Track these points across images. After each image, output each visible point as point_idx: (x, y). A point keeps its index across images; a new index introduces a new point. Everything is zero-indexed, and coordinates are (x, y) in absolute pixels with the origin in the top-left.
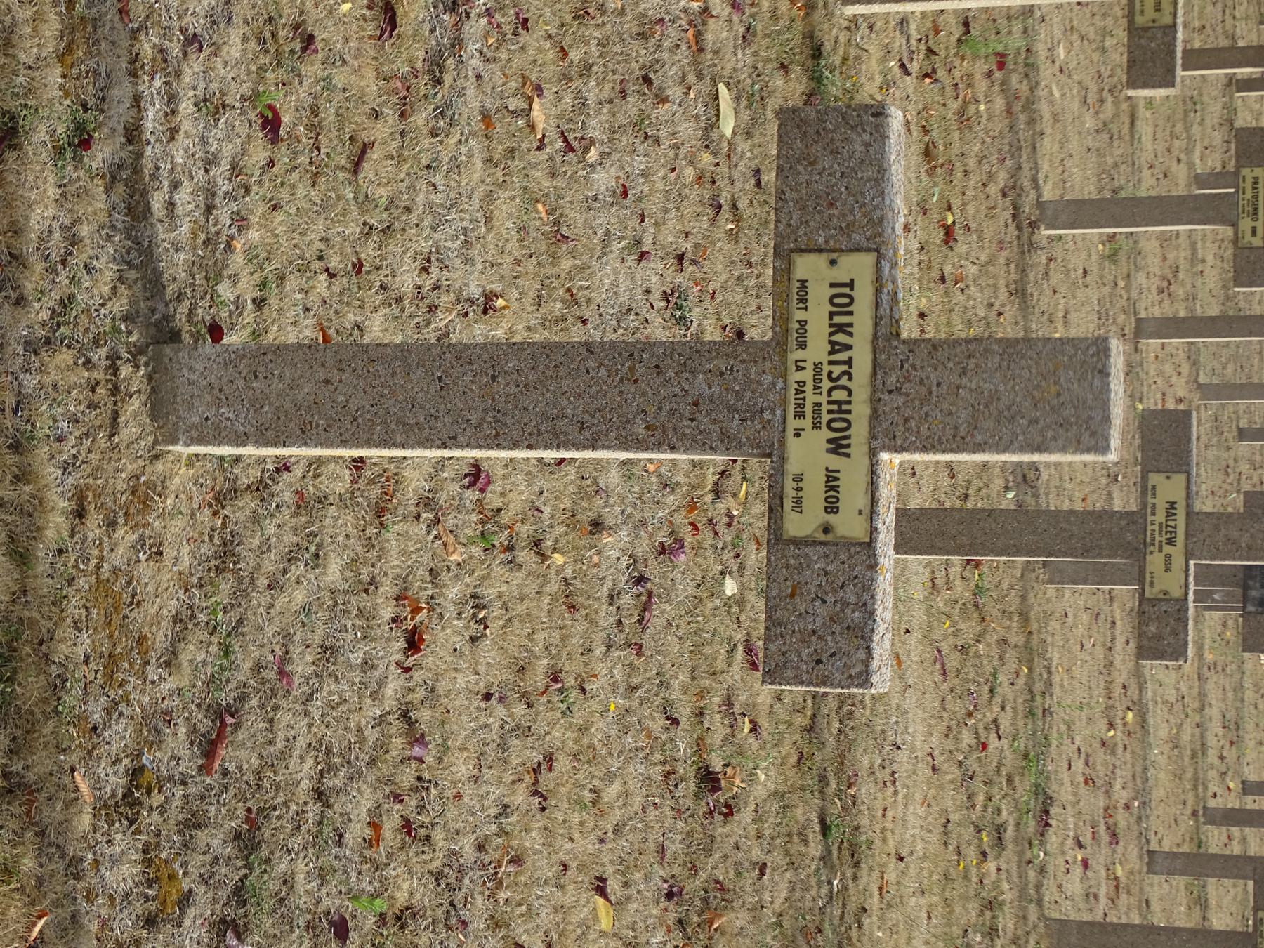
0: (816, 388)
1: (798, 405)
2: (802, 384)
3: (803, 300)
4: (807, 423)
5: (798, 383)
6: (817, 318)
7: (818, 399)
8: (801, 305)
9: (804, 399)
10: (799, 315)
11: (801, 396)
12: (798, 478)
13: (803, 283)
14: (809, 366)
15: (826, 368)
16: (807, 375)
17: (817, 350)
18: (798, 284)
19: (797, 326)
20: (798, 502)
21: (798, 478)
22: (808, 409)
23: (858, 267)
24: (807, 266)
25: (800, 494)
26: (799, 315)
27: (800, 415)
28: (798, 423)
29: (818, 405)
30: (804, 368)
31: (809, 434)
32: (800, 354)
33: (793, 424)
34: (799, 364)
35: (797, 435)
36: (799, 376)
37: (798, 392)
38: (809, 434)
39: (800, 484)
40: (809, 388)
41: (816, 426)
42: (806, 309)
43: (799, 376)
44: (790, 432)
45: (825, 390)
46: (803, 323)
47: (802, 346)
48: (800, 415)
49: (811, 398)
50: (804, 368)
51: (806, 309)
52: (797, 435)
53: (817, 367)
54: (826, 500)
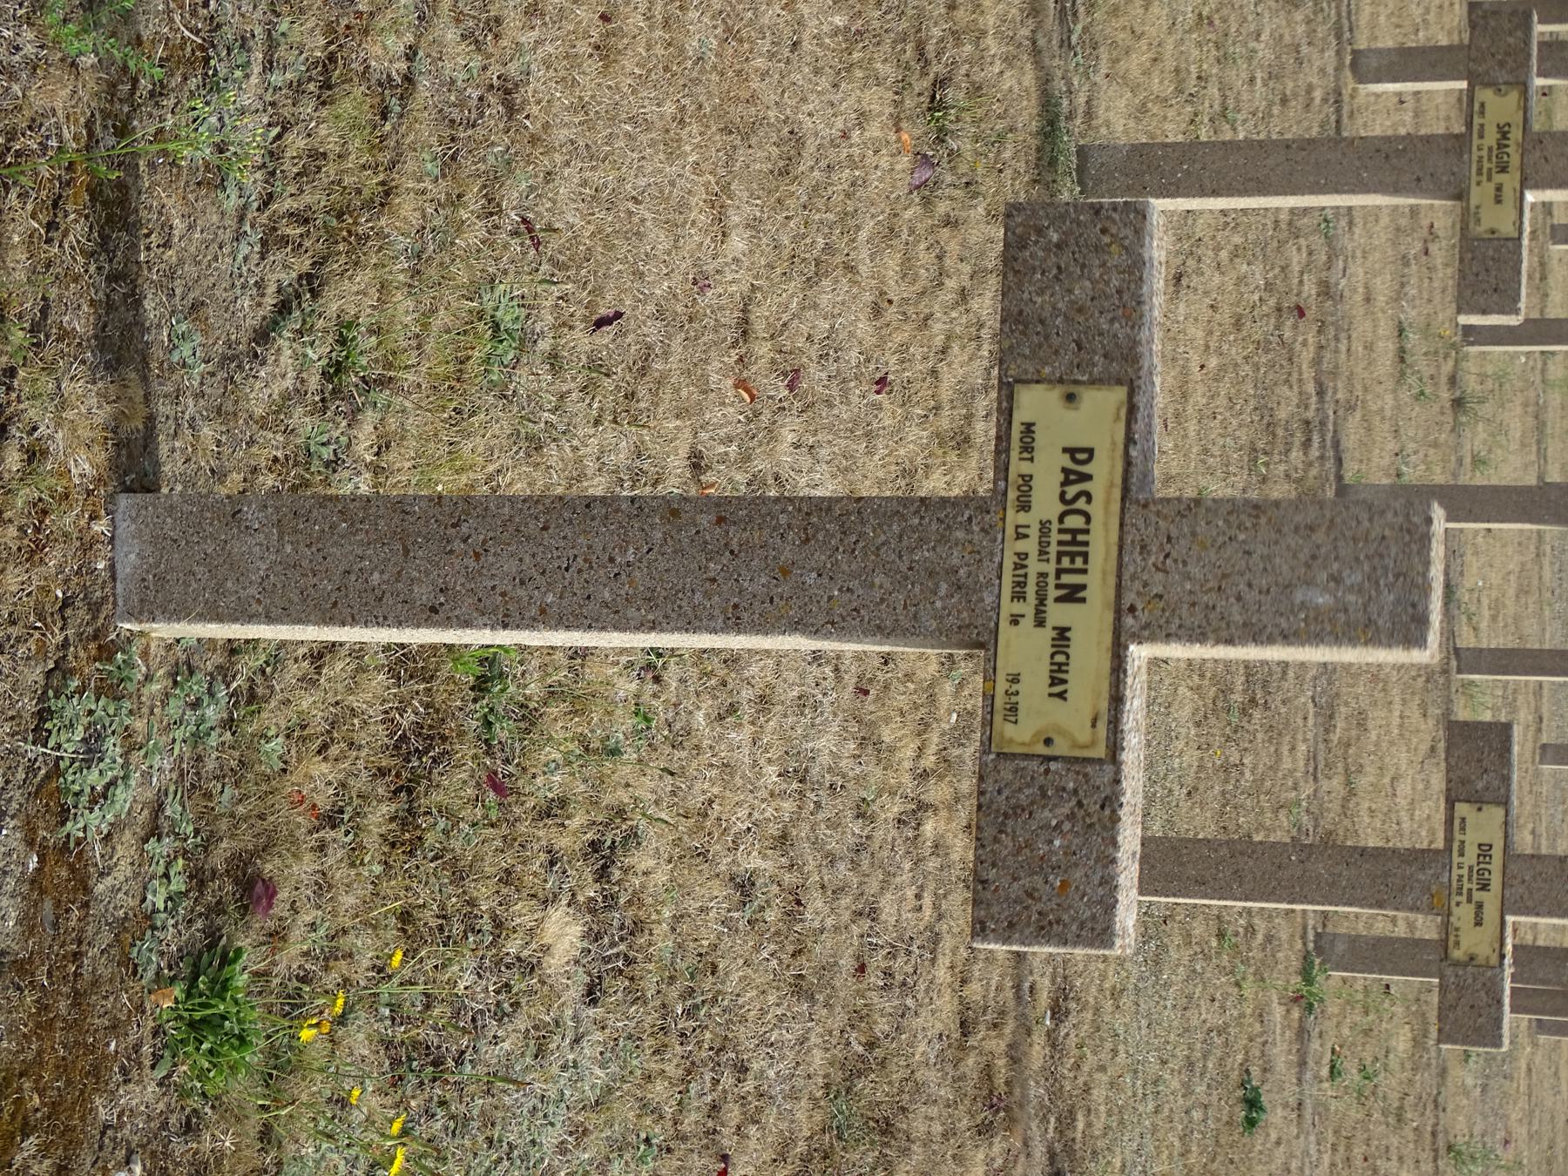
1: (1018, 584)
2: (1023, 556)
3: (1028, 448)
5: (1018, 554)
6: (1046, 471)
8: (1026, 455)
9: (1025, 576)
12: (1015, 679)
13: (1029, 428)
18: (1023, 428)
19: (1020, 481)
20: (1013, 709)
21: (1015, 679)
24: (1034, 403)
25: (1014, 699)
26: (1025, 468)
30: (1026, 536)
32: (1022, 518)
33: (1008, 607)
34: (1020, 530)
37: (1017, 566)
39: (1015, 687)
42: (1032, 459)
43: (1021, 546)
44: (1004, 624)
46: (1027, 479)
50: (1026, 536)
51: (1032, 459)
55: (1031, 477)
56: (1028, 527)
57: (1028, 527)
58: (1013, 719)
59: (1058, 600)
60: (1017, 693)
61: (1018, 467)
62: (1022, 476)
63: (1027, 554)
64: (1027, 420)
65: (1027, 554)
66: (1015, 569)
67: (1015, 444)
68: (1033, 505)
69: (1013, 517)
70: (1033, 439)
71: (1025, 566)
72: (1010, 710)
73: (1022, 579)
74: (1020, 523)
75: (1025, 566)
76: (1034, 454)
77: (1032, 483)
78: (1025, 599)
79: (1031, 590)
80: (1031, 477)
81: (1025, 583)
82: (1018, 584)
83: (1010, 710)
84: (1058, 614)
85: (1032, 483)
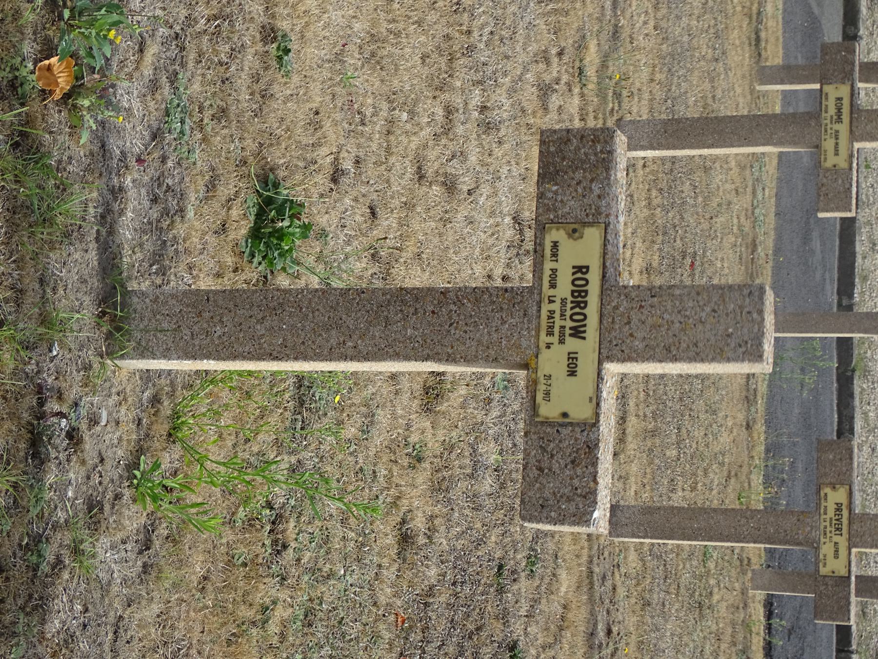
0: (562, 315)
2: (552, 312)
3: (555, 255)
4: (555, 339)
5: (550, 311)
7: (563, 323)
8: (554, 258)
9: (554, 323)
10: (553, 265)
11: (552, 320)
14: (558, 301)
15: (569, 301)
16: (556, 306)
17: (564, 289)
18: (552, 244)
19: (550, 272)
20: (547, 394)
22: (556, 330)
23: (593, 235)
26: (553, 265)
27: (550, 333)
28: (549, 339)
29: (563, 327)
31: (556, 347)
32: (552, 292)
33: (544, 338)
35: (548, 347)
36: (552, 307)
37: (549, 318)
38: (556, 347)
39: (549, 382)
40: (557, 315)
41: (562, 342)
42: (557, 261)
43: (552, 307)
45: (568, 317)
46: (554, 271)
47: (553, 286)
48: (550, 333)
49: (558, 323)
50: (554, 301)
51: (557, 261)
52: (548, 347)
53: (563, 301)
54: (568, 366)
55: (556, 270)
56: (555, 296)
57: (555, 296)
58: (548, 399)
59: (571, 335)
60: (550, 385)
61: (548, 266)
62: (552, 270)
63: (554, 311)
64: (556, 240)
65: (554, 311)
66: (548, 319)
67: (548, 252)
68: (558, 285)
69: (547, 291)
70: (558, 250)
71: (553, 318)
72: (546, 394)
73: (552, 324)
74: (550, 295)
75: (553, 318)
76: (559, 258)
77: (557, 273)
78: (553, 335)
79: (556, 330)
80: (556, 270)
81: (554, 327)
82: (550, 327)
83: (546, 394)
84: (572, 344)
85: (557, 273)
